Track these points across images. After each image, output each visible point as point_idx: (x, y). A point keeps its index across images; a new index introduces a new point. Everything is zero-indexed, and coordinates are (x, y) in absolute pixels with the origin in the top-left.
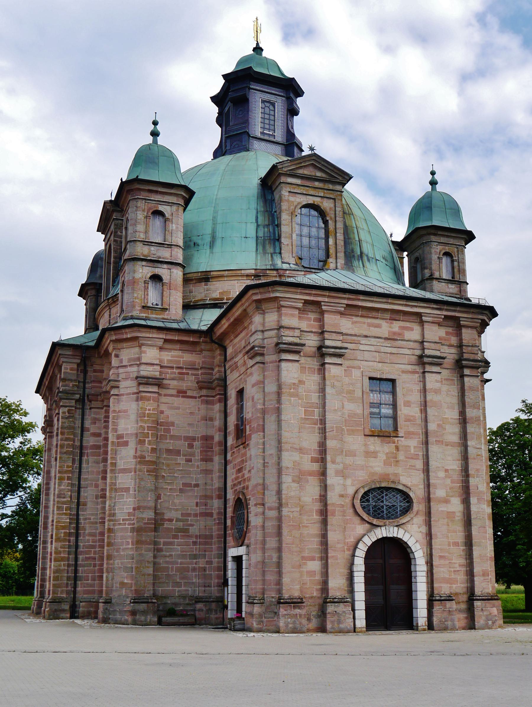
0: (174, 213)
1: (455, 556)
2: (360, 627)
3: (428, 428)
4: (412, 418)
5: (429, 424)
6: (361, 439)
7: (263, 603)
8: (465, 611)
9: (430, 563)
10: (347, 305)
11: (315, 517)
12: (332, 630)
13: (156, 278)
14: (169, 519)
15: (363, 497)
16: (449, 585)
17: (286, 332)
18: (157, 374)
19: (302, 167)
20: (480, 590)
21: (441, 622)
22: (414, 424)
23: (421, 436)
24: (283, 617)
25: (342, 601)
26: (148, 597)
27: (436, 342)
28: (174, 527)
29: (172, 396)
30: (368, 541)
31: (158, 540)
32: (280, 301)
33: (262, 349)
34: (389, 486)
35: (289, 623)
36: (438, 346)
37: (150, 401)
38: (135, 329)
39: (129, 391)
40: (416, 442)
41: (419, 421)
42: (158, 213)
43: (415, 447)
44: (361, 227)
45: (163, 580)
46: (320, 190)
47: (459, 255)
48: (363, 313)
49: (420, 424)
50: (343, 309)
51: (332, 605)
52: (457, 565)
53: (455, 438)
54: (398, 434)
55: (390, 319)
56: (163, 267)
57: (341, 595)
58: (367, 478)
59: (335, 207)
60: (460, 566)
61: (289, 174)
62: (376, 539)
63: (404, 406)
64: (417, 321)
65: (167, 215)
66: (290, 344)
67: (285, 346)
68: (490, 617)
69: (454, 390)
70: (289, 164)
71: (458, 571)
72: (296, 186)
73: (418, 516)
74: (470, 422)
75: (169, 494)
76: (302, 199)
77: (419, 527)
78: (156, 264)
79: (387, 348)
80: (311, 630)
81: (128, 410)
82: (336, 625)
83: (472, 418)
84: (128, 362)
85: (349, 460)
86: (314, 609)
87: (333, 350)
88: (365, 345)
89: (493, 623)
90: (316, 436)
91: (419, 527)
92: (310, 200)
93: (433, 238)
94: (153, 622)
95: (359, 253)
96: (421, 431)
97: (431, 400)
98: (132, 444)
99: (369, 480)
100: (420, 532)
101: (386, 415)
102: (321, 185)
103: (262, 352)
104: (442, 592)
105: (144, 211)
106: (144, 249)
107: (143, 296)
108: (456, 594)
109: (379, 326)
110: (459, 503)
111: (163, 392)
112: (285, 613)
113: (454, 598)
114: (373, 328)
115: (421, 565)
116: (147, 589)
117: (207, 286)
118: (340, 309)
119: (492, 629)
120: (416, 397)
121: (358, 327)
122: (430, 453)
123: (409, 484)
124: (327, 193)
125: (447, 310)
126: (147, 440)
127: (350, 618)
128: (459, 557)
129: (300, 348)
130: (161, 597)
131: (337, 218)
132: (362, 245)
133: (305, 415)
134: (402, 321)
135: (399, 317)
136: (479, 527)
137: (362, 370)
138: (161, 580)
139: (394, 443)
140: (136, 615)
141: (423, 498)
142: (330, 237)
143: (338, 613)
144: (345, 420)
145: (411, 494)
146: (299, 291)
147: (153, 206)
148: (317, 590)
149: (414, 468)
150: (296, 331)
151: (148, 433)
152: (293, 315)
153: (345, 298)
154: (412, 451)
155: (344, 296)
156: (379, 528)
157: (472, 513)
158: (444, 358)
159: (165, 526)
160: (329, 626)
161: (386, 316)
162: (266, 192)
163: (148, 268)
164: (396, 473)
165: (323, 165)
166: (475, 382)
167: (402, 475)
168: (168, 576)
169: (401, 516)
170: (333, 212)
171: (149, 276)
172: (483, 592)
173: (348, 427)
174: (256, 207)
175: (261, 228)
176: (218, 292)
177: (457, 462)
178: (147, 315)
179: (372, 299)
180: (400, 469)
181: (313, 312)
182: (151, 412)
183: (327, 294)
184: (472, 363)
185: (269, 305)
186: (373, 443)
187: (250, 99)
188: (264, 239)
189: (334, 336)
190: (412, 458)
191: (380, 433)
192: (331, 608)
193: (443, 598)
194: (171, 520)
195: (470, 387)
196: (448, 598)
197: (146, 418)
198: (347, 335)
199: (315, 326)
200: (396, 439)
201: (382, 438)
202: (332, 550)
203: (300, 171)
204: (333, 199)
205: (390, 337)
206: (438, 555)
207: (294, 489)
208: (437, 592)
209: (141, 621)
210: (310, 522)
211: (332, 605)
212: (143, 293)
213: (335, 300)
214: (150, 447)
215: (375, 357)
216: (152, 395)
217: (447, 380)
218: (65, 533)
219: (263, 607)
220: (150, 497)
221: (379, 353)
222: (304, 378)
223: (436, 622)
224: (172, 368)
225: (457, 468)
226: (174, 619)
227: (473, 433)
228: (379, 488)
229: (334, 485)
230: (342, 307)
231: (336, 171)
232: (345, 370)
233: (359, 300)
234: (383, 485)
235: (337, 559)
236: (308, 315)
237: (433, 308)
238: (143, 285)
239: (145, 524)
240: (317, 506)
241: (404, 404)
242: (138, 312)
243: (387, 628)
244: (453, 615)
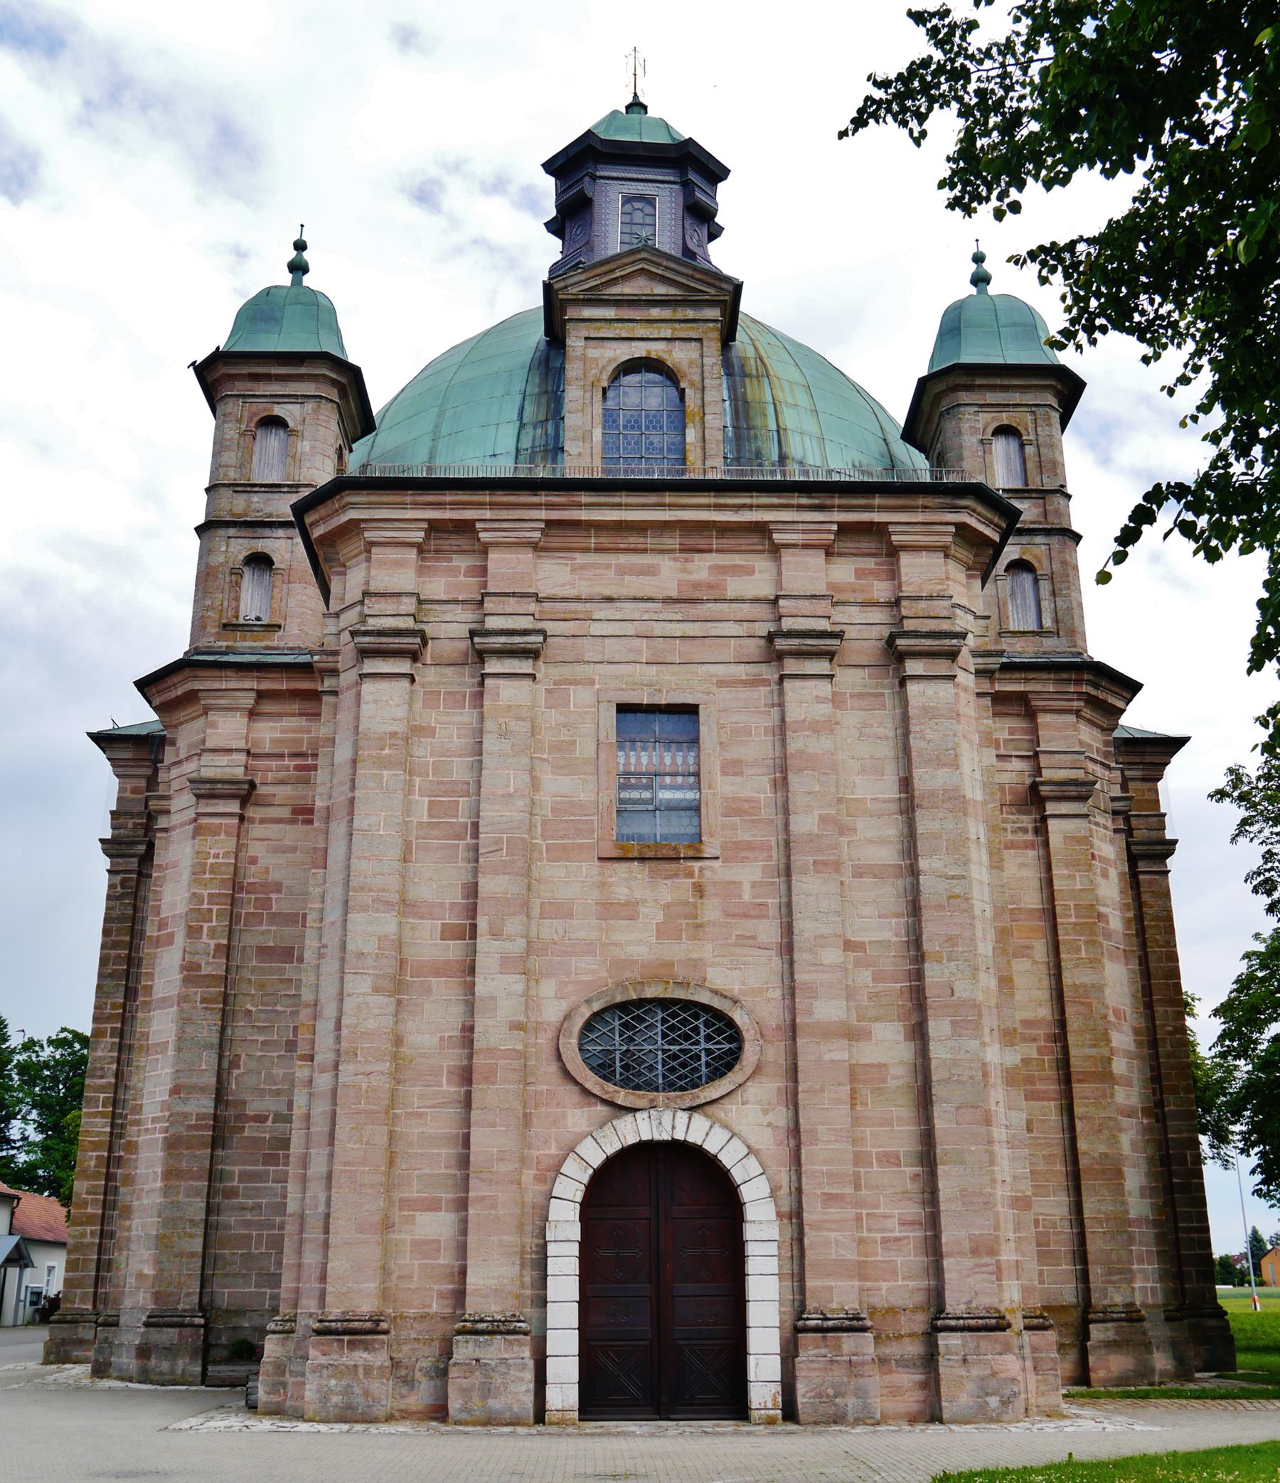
1: (886, 1196)
2: (560, 1407)
3: (792, 828)
4: (746, 806)
5: (792, 818)
6: (588, 869)
7: (292, 1331)
8: (918, 1363)
9: (794, 1217)
10: (550, 524)
11: (445, 1088)
12: (464, 1416)
13: (261, 561)
14: (256, 1116)
16: (857, 1284)
17: (377, 606)
18: (239, 773)
19: (617, 279)
20: (965, 1300)
21: (821, 1396)
22: (753, 821)
23: (774, 854)
24: (314, 1372)
26: (185, 1311)
27: (814, 597)
28: (267, 1136)
31: (227, 1168)
32: (365, 529)
33: (331, 658)
34: (668, 996)
35: (331, 1391)
36: (823, 607)
37: (219, 834)
38: (187, 672)
40: (759, 870)
41: (768, 813)
42: (277, 423)
43: (754, 885)
44: (790, 400)
45: (235, 1269)
46: (664, 325)
47: (1039, 429)
48: (601, 540)
49: (772, 821)
50: (537, 534)
51: (467, 1342)
52: (893, 1223)
53: (889, 855)
54: (699, 851)
55: (681, 551)
56: (275, 535)
57: (503, 1312)
58: (605, 974)
59: (702, 356)
60: (902, 1224)
61: (583, 300)
62: (618, 1147)
63: (724, 773)
64: (760, 547)
65: (291, 424)
66: (380, 633)
67: (367, 639)
68: (993, 1383)
69: (884, 723)
70: (583, 277)
71: (897, 1239)
72: (603, 324)
73: (764, 1079)
74: (925, 803)
75: (259, 1054)
76: (618, 351)
77: (765, 1112)
78: (259, 530)
79: (673, 625)
80: (415, 1413)
83: (932, 793)
85: (549, 930)
86: (427, 1351)
87: (503, 639)
88: (604, 621)
89: (1005, 1403)
90: (460, 868)
91: (765, 1112)
93: (964, 397)
94: (191, 1375)
95: (775, 457)
96: (773, 839)
97: (801, 753)
98: (180, 939)
99: (610, 981)
100: (769, 1125)
101: (674, 804)
102: (666, 313)
103: (331, 665)
104: (834, 1306)
105: (239, 421)
106: (235, 502)
108: (892, 1311)
109: (651, 571)
110: (901, 1037)
112: (323, 1360)
113: (869, 1323)
114: (633, 578)
115: (761, 1222)
116: (185, 1291)
118: (528, 534)
119: (998, 1421)
120: (760, 748)
121: (589, 579)
122: (794, 898)
123: (736, 989)
124: (681, 329)
125: (843, 508)
126: (206, 926)
127: (521, 1379)
128: (900, 1197)
130: (228, 1311)
131: (707, 382)
132: (787, 441)
133: (430, 816)
134: (718, 551)
135: (708, 541)
136: (958, 1108)
137: (597, 686)
138: (228, 1269)
139: (690, 875)
140: (148, 1358)
141: (779, 1028)
142: (690, 425)
143: (485, 1364)
144: (544, 823)
145: (738, 1017)
146: (408, 499)
147: (262, 409)
148: (441, 1295)
149: (750, 942)
150: (405, 600)
151: (211, 910)
152: (400, 564)
153: (540, 505)
154: (747, 896)
155: (535, 499)
157: (933, 1065)
158: (839, 635)
159: (246, 1134)
161: (670, 541)
162: (552, 353)
163: (240, 541)
164: (694, 960)
165: (667, 268)
166: (942, 694)
167: (712, 966)
168: (247, 1257)
169: (710, 1079)
170: (698, 370)
171: (241, 557)
172: (974, 1305)
173: (552, 838)
175: (529, 429)
177: (893, 921)
178: (230, 644)
179: (616, 500)
180: (709, 946)
181: (463, 552)
182: (221, 860)
183: (487, 499)
184: (929, 642)
185: (349, 549)
186: (626, 880)
187: (596, 199)
189: (512, 605)
190: (746, 916)
191: (645, 850)
192: (464, 1350)
193: (830, 1323)
194: (261, 1119)
196: (847, 1323)
197: (207, 876)
198: (552, 599)
199: (467, 587)
200: (696, 865)
201: (653, 864)
202: (482, 1179)
203: (615, 290)
204: (696, 340)
206: (819, 1192)
207: (376, 1011)
208: (816, 1305)
209: (161, 1373)
210: (429, 1103)
211: (467, 1342)
213: (511, 512)
214: (212, 943)
215: (639, 651)
217: (860, 696)
218: (98, 1157)
219: (289, 1342)
220: (208, 1062)
221: (652, 642)
222: (431, 718)
223: (804, 1396)
224: (280, 756)
225: (894, 939)
226: (238, 1368)
227: (937, 836)
228: (640, 1003)
229: (494, 998)
230: (535, 529)
231: (698, 276)
232: (548, 691)
233: (580, 506)
234: (650, 993)
235: (494, 1207)
236: (450, 560)
237: (800, 507)
239: (190, 1127)
240: (452, 1058)
241: (722, 768)
242: (212, 639)
243: (659, 1413)
244: (862, 1376)
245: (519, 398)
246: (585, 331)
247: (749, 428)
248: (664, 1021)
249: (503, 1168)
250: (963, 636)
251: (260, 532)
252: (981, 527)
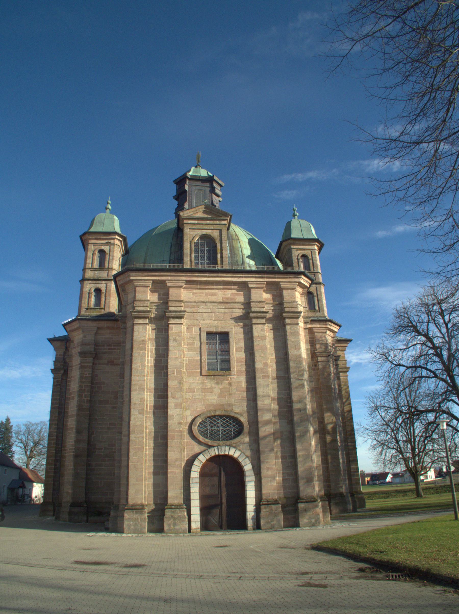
15: (200, 423)
25: (178, 507)
30: (203, 459)
32: (135, 282)
54: (230, 373)
79: (222, 310)
82: (172, 526)
87: (174, 313)
92: (204, 232)
95: (242, 262)
102: (211, 222)
104: (270, 498)
114: (210, 296)
125: (267, 278)
129: (148, 314)
139: (228, 380)
151: (85, 390)
156: (213, 449)
160: (166, 528)
167: (234, 405)
184: (292, 314)
193: (269, 503)
195: (291, 333)
205: (224, 301)
225: (284, 397)
228: (214, 416)
229: (173, 415)
234: (217, 413)
237: (256, 277)
246: (189, 226)
247: (234, 254)
248: (221, 421)
249: (177, 463)
250: (301, 312)
251: (98, 282)
252: (304, 283)
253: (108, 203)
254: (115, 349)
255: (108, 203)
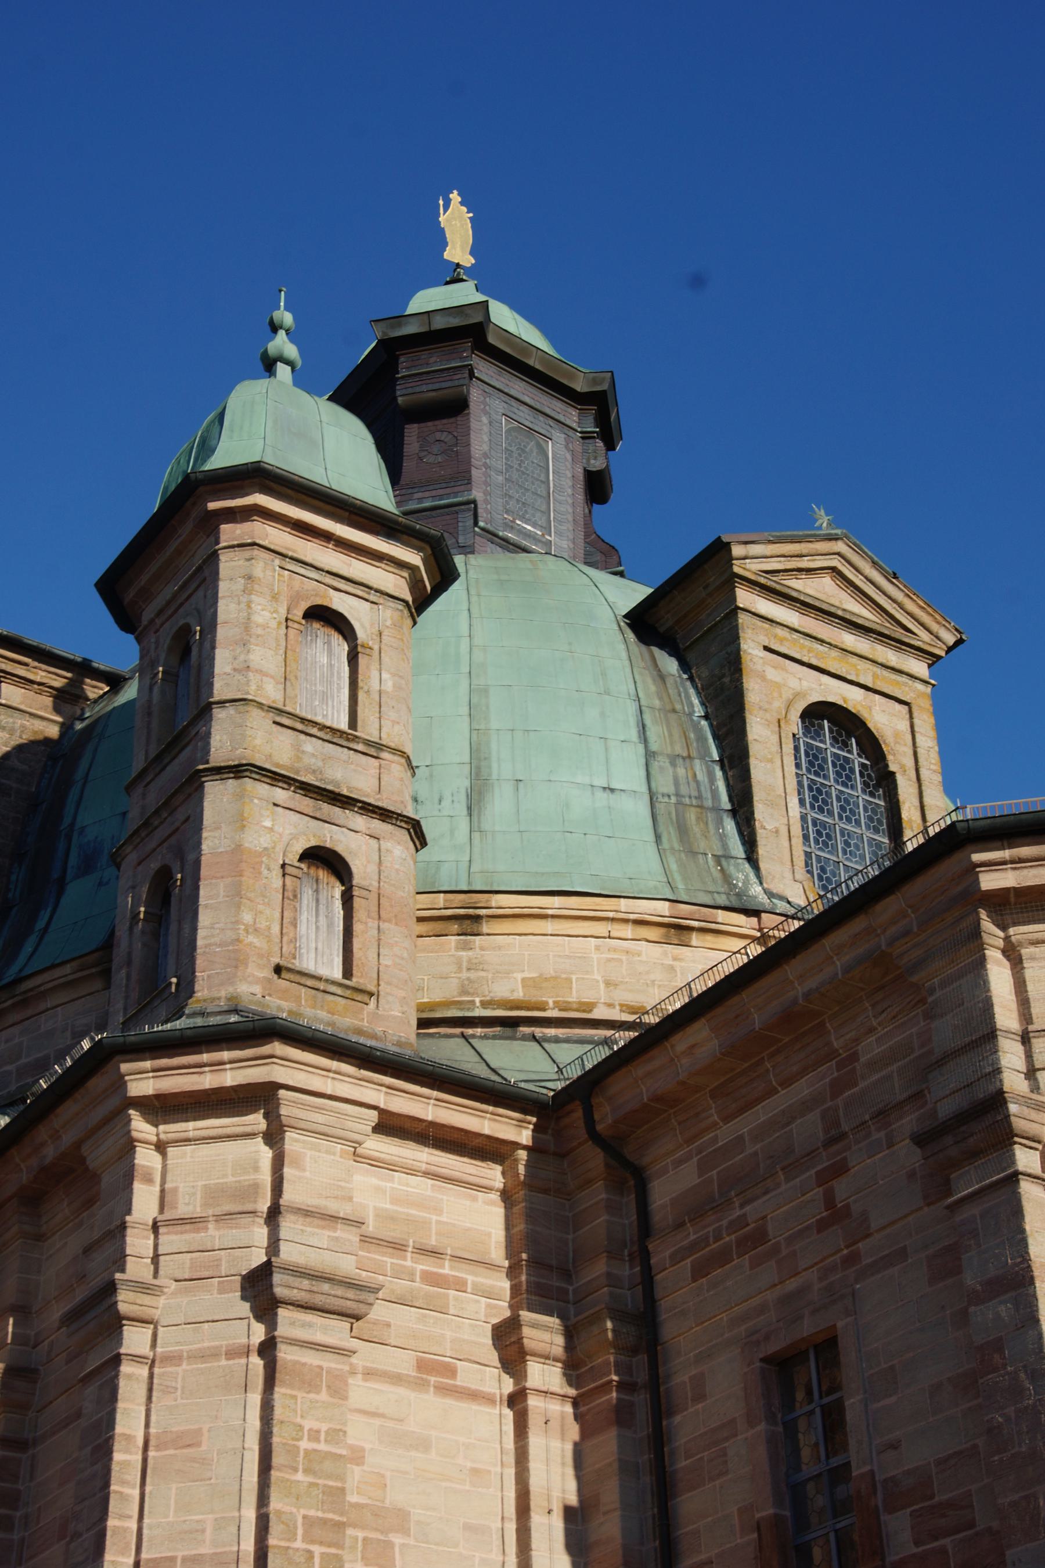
0: (385, 633)
29: (396, 1379)
37: (317, 1390)
39: (209, 1338)
76: (805, 684)
81: (199, 1432)
84: (205, 1205)
105: (275, 597)
107: (276, 929)
111: (367, 1355)
117: (470, 953)
151: (310, 1555)
171: (300, 846)
174: (633, 691)
176: (519, 976)
182: (322, 1447)
188: (678, 803)
197: (300, 1476)
212: (278, 915)
216: (325, 1365)
224: (398, 1247)
238: (277, 883)
245: (632, 708)
253: (274, 328)
254: (460, 1286)
255: (274, 328)
